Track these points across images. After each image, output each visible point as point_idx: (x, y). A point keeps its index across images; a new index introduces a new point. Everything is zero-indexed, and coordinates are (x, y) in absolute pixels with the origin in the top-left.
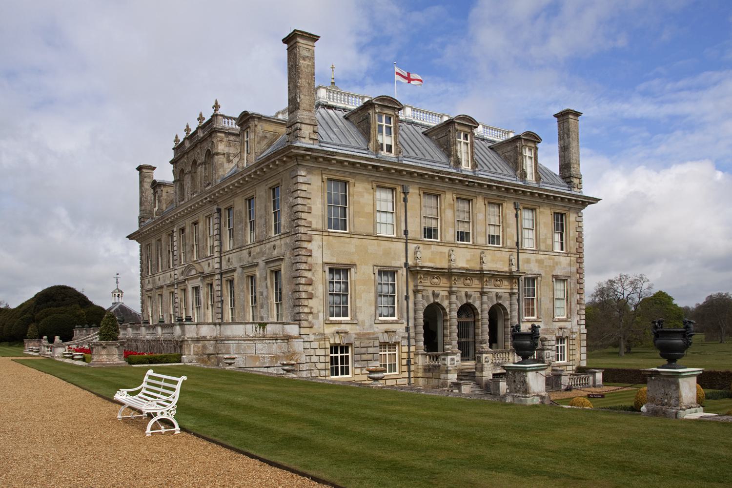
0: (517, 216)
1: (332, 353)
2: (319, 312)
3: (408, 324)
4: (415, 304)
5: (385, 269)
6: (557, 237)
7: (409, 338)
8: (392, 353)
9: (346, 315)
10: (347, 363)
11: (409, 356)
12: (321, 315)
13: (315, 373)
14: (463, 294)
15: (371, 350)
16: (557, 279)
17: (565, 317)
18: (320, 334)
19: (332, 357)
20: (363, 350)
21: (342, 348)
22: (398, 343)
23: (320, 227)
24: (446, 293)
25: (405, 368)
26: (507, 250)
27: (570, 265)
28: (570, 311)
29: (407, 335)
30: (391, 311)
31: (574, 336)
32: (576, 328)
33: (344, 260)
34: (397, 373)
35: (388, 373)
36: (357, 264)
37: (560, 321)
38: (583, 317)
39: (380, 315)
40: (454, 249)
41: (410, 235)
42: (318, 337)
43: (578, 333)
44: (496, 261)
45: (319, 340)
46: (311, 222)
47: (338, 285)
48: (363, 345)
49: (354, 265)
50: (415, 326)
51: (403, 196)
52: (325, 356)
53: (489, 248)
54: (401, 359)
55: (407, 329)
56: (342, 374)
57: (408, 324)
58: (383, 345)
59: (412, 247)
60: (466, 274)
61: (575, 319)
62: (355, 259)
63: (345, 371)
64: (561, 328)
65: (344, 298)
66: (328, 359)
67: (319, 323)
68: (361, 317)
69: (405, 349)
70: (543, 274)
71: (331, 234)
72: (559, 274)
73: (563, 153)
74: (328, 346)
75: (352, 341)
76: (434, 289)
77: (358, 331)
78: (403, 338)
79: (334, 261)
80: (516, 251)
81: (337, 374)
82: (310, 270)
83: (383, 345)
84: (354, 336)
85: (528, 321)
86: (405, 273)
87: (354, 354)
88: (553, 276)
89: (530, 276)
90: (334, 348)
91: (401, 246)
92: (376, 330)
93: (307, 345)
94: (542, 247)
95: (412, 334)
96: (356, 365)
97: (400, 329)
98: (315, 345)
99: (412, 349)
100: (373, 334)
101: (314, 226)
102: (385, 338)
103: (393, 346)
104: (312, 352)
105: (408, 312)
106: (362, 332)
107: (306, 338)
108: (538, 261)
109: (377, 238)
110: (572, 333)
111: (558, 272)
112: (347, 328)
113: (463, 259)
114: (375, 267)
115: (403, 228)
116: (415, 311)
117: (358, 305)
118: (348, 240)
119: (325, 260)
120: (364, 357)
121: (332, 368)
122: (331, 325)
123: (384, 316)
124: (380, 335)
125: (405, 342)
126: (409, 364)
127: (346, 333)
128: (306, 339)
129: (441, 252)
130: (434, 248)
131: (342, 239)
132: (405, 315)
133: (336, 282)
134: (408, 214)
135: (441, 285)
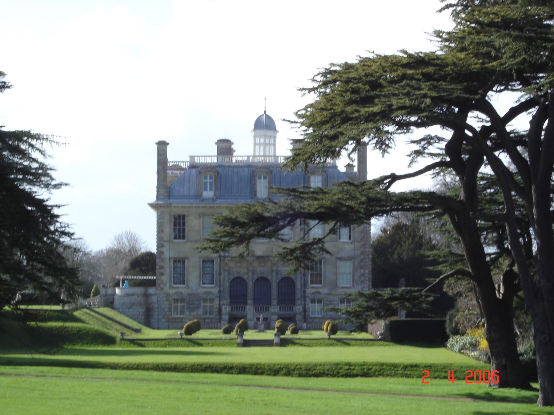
5: (206, 259)
7: (220, 297)
12: (168, 284)
16: (340, 259)
25: (217, 313)
49: (187, 258)
55: (220, 292)
58: (205, 300)
67: (167, 288)
69: (217, 302)
79: (176, 256)
85: (312, 287)
97: (215, 291)
101: (165, 239)
103: (212, 300)
112: (183, 291)
127: (181, 293)
132: (218, 283)
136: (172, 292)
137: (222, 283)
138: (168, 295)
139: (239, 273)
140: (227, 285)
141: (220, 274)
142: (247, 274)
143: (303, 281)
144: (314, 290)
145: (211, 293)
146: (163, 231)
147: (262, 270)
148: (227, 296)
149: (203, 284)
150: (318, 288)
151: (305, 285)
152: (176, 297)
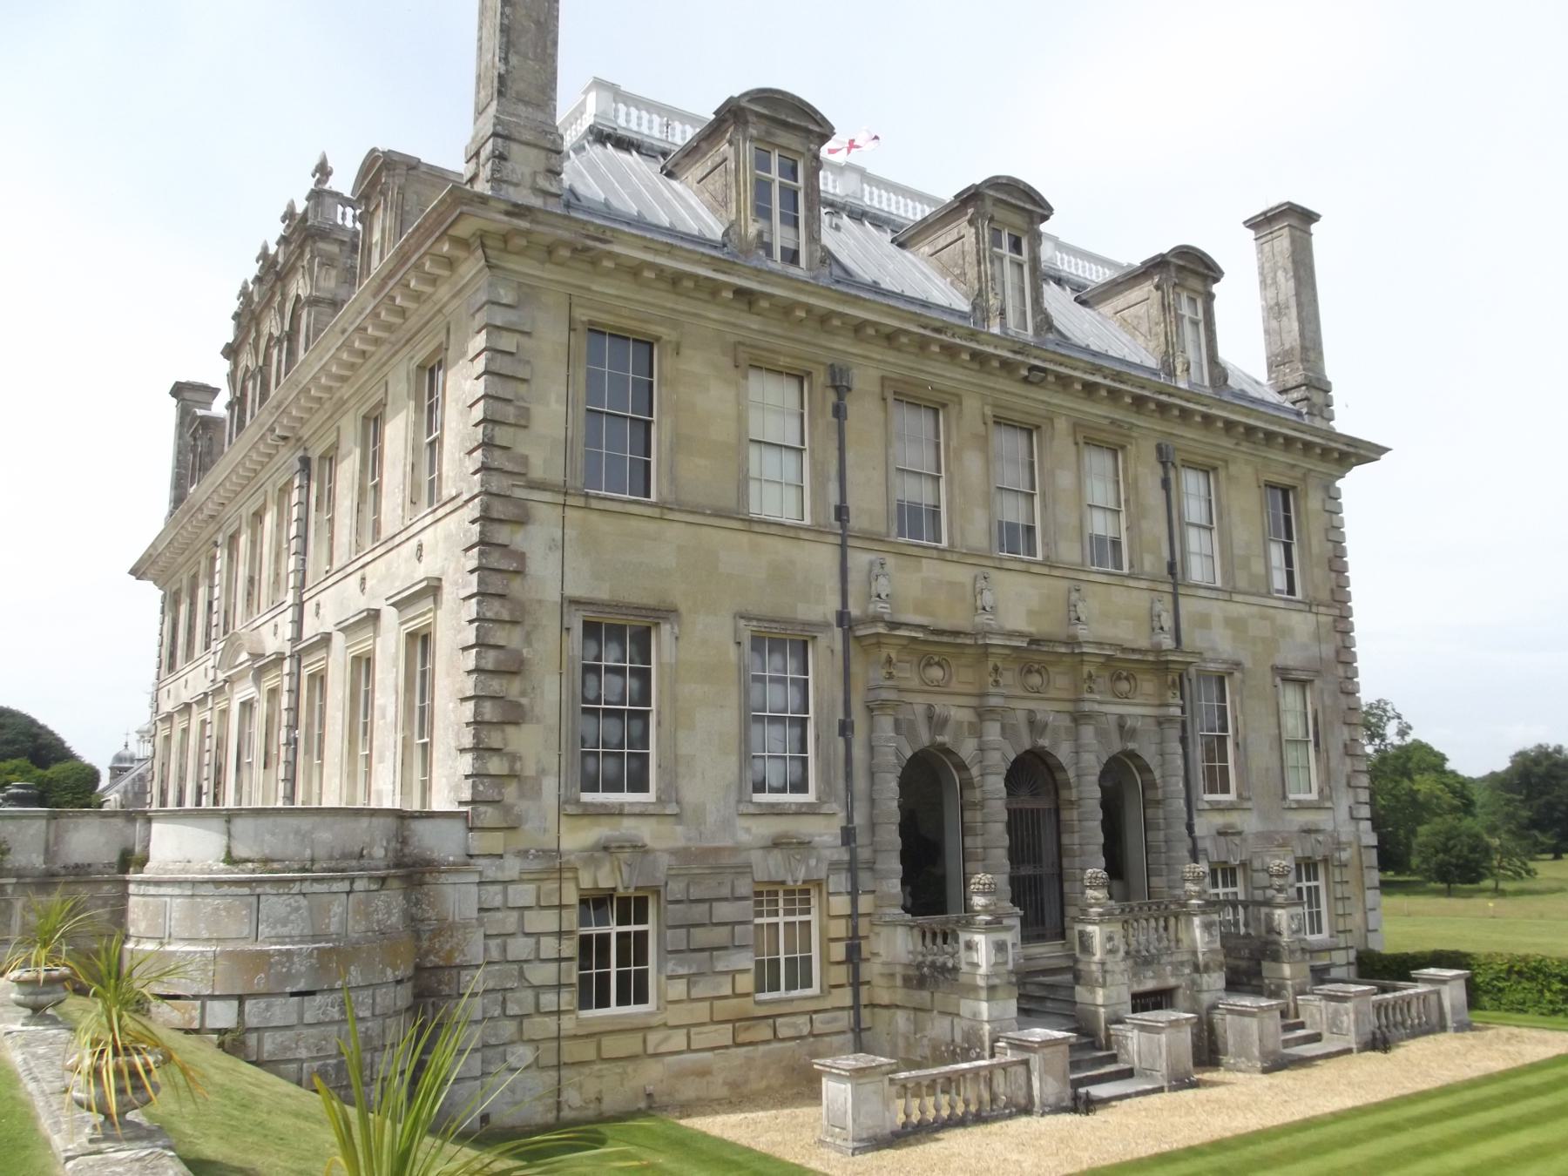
0: (1166, 484)
1: (584, 922)
2: (543, 772)
3: (850, 818)
4: (871, 749)
5: (776, 630)
6: (1277, 553)
7: (852, 868)
8: (797, 918)
9: (640, 784)
10: (642, 958)
11: (855, 928)
12: (550, 785)
13: (519, 1002)
14: (1021, 717)
15: (724, 911)
16: (1284, 675)
17: (1314, 796)
18: (544, 853)
19: (585, 941)
20: (699, 912)
21: (624, 902)
22: (819, 884)
23: (557, 476)
24: (965, 716)
25: (840, 974)
26: (1143, 584)
27: (1318, 638)
28: (1327, 775)
29: (846, 857)
30: (793, 770)
31: (1345, 856)
32: (1346, 831)
33: (637, 592)
34: (816, 989)
35: (782, 993)
36: (683, 608)
37: (1303, 806)
38: (1364, 796)
39: (759, 787)
40: (994, 574)
41: (856, 522)
42: (536, 865)
43: (1355, 846)
44: (1116, 616)
45: (537, 878)
46: (524, 460)
47: (616, 680)
48: (695, 893)
49: (666, 613)
50: (873, 826)
51: (832, 397)
52: (560, 934)
53: (1092, 577)
54: (827, 940)
55: (848, 835)
56: (623, 1000)
57: (850, 818)
58: (765, 895)
59: (859, 560)
60: (1033, 655)
61: (1344, 801)
62: (677, 594)
63: (633, 990)
64: (1308, 831)
65: (637, 725)
66: (570, 948)
68: (692, 792)
69: (841, 905)
70: (1248, 664)
71: (594, 504)
72: (1290, 663)
73: (1274, 324)
74: (571, 897)
75: (661, 876)
76: (933, 699)
77: (681, 843)
78: (834, 866)
79: (603, 594)
80: (1168, 588)
81: (603, 1002)
82: (514, 623)
83: (765, 895)
84: (664, 861)
86: (839, 646)
87: (663, 927)
88: (1277, 670)
89: (1212, 666)
90: (596, 903)
91: (823, 556)
92: (744, 838)
93: (494, 896)
94: (1242, 583)
95: (864, 854)
96: (670, 967)
97: (825, 832)
98: (524, 894)
99: (865, 904)
100: (736, 850)
101: (537, 472)
102: (770, 866)
104: (510, 921)
105: (849, 776)
106: (693, 845)
107: (491, 870)
108: (1232, 623)
109: (752, 524)
110: (1339, 846)
111: (1289, 657)
112: (645, 831)
113: (1018, 603)
114: (742, 623)
115: (834, 498)
116: (872, 775)
117: (684, 749)
118: (652, 527)
119: (572, 591)
120: (701, 937)
121: (584, 981)
122: (585, 821)
123: (773, 790)
124: (756, 857)
125: (839, 882)
126: (854, 956)
127: (640, 849)
128: (491, 874)
129: (951, 583)
130: (931, 569)
131: (634, 523)
132: (840, 784)
133: (609, 670)
134: (850, 457)
135: (955, 686)
136: (577, 838)
137: (860, 783)
138: (554, 865)
141: (846, 728)
142: (976, 731)
145: (804, 845)
146: (522, 423)
152: (606, 878)
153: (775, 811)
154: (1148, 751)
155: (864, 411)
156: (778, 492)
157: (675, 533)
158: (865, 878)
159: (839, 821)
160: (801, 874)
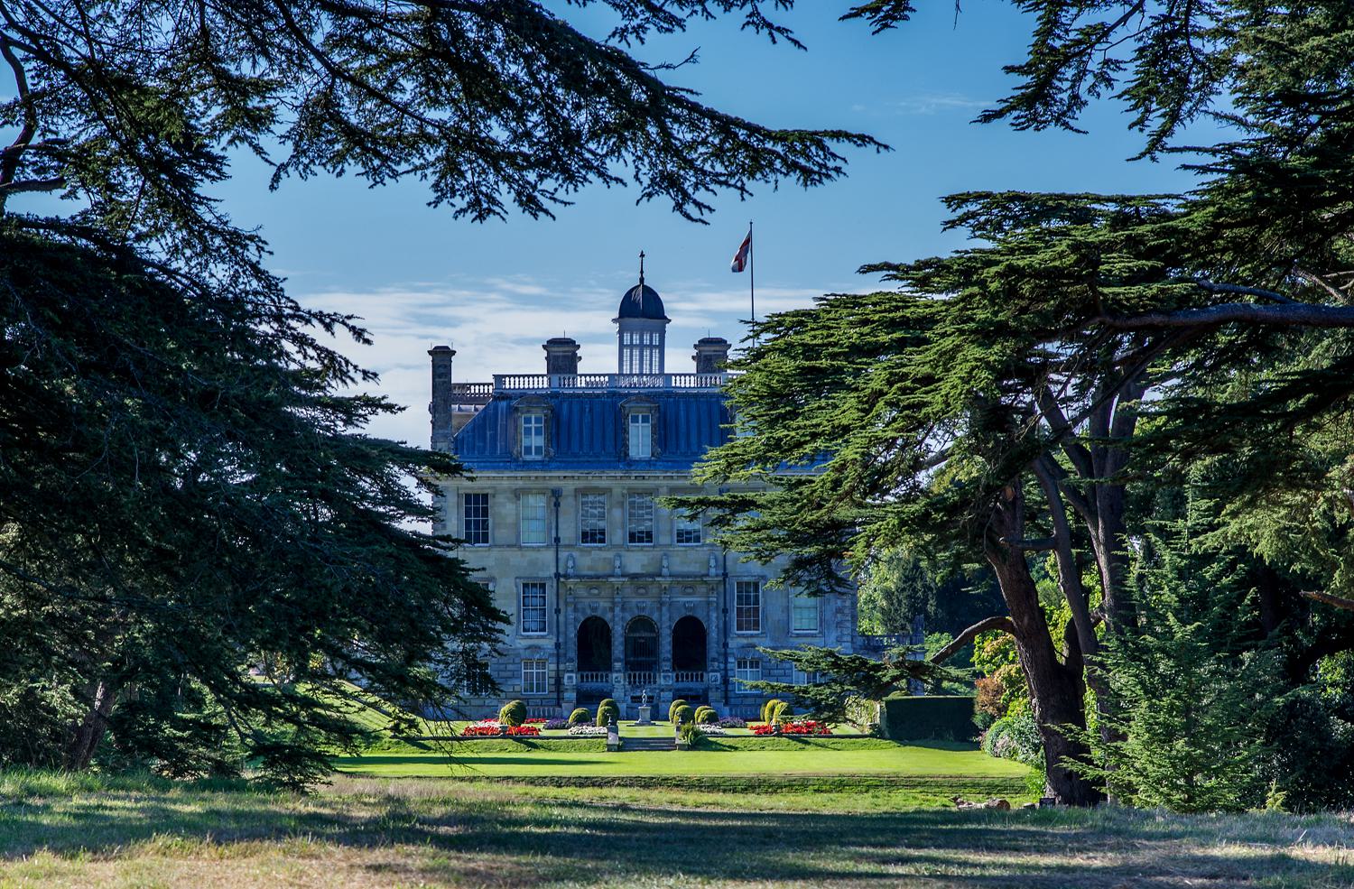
7: (558, 656)
20: (502, 667)
25: (553, 688)
40: (623, 553)
41: (562, 543)
55: (558, 645)
59: (563, 555)
69: (553, 667)
78: (550, 655)
85: (739, 636)
89: (746, 579)
91: (549, 555)
97: (548, 643)
109: (521, 548)
113: (637, 560)
115: (554, 535)
125: (555, 660)
126: (558, 681)
132: (555, 629)
134: (560, 520)
137: (562, 629)
139: (595, 609)
140: (572, 634)
141: (558, 611)
142: (612, 610)
143: (721, 625)
144: (745, 641)
145: (538, 648)
147: (644, 603)
148: (573, 654)
149: (525, 630)
150: (752, 636)
151: (725, 631)
153: (528, 637)
154: (700, 615)
155: (567, 504)
156: (534, 534)
157: (495, 553)
158: (562, 659)
159: (554, 640)
160: (537, 656)
